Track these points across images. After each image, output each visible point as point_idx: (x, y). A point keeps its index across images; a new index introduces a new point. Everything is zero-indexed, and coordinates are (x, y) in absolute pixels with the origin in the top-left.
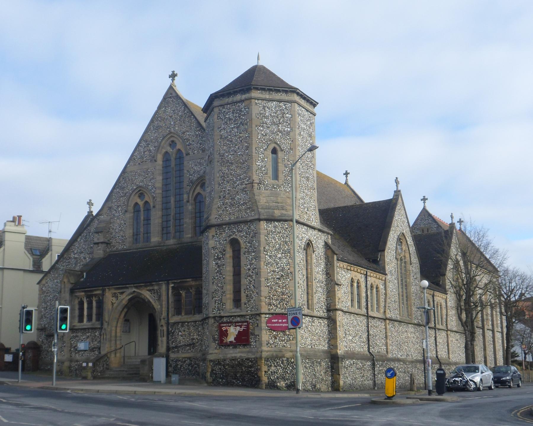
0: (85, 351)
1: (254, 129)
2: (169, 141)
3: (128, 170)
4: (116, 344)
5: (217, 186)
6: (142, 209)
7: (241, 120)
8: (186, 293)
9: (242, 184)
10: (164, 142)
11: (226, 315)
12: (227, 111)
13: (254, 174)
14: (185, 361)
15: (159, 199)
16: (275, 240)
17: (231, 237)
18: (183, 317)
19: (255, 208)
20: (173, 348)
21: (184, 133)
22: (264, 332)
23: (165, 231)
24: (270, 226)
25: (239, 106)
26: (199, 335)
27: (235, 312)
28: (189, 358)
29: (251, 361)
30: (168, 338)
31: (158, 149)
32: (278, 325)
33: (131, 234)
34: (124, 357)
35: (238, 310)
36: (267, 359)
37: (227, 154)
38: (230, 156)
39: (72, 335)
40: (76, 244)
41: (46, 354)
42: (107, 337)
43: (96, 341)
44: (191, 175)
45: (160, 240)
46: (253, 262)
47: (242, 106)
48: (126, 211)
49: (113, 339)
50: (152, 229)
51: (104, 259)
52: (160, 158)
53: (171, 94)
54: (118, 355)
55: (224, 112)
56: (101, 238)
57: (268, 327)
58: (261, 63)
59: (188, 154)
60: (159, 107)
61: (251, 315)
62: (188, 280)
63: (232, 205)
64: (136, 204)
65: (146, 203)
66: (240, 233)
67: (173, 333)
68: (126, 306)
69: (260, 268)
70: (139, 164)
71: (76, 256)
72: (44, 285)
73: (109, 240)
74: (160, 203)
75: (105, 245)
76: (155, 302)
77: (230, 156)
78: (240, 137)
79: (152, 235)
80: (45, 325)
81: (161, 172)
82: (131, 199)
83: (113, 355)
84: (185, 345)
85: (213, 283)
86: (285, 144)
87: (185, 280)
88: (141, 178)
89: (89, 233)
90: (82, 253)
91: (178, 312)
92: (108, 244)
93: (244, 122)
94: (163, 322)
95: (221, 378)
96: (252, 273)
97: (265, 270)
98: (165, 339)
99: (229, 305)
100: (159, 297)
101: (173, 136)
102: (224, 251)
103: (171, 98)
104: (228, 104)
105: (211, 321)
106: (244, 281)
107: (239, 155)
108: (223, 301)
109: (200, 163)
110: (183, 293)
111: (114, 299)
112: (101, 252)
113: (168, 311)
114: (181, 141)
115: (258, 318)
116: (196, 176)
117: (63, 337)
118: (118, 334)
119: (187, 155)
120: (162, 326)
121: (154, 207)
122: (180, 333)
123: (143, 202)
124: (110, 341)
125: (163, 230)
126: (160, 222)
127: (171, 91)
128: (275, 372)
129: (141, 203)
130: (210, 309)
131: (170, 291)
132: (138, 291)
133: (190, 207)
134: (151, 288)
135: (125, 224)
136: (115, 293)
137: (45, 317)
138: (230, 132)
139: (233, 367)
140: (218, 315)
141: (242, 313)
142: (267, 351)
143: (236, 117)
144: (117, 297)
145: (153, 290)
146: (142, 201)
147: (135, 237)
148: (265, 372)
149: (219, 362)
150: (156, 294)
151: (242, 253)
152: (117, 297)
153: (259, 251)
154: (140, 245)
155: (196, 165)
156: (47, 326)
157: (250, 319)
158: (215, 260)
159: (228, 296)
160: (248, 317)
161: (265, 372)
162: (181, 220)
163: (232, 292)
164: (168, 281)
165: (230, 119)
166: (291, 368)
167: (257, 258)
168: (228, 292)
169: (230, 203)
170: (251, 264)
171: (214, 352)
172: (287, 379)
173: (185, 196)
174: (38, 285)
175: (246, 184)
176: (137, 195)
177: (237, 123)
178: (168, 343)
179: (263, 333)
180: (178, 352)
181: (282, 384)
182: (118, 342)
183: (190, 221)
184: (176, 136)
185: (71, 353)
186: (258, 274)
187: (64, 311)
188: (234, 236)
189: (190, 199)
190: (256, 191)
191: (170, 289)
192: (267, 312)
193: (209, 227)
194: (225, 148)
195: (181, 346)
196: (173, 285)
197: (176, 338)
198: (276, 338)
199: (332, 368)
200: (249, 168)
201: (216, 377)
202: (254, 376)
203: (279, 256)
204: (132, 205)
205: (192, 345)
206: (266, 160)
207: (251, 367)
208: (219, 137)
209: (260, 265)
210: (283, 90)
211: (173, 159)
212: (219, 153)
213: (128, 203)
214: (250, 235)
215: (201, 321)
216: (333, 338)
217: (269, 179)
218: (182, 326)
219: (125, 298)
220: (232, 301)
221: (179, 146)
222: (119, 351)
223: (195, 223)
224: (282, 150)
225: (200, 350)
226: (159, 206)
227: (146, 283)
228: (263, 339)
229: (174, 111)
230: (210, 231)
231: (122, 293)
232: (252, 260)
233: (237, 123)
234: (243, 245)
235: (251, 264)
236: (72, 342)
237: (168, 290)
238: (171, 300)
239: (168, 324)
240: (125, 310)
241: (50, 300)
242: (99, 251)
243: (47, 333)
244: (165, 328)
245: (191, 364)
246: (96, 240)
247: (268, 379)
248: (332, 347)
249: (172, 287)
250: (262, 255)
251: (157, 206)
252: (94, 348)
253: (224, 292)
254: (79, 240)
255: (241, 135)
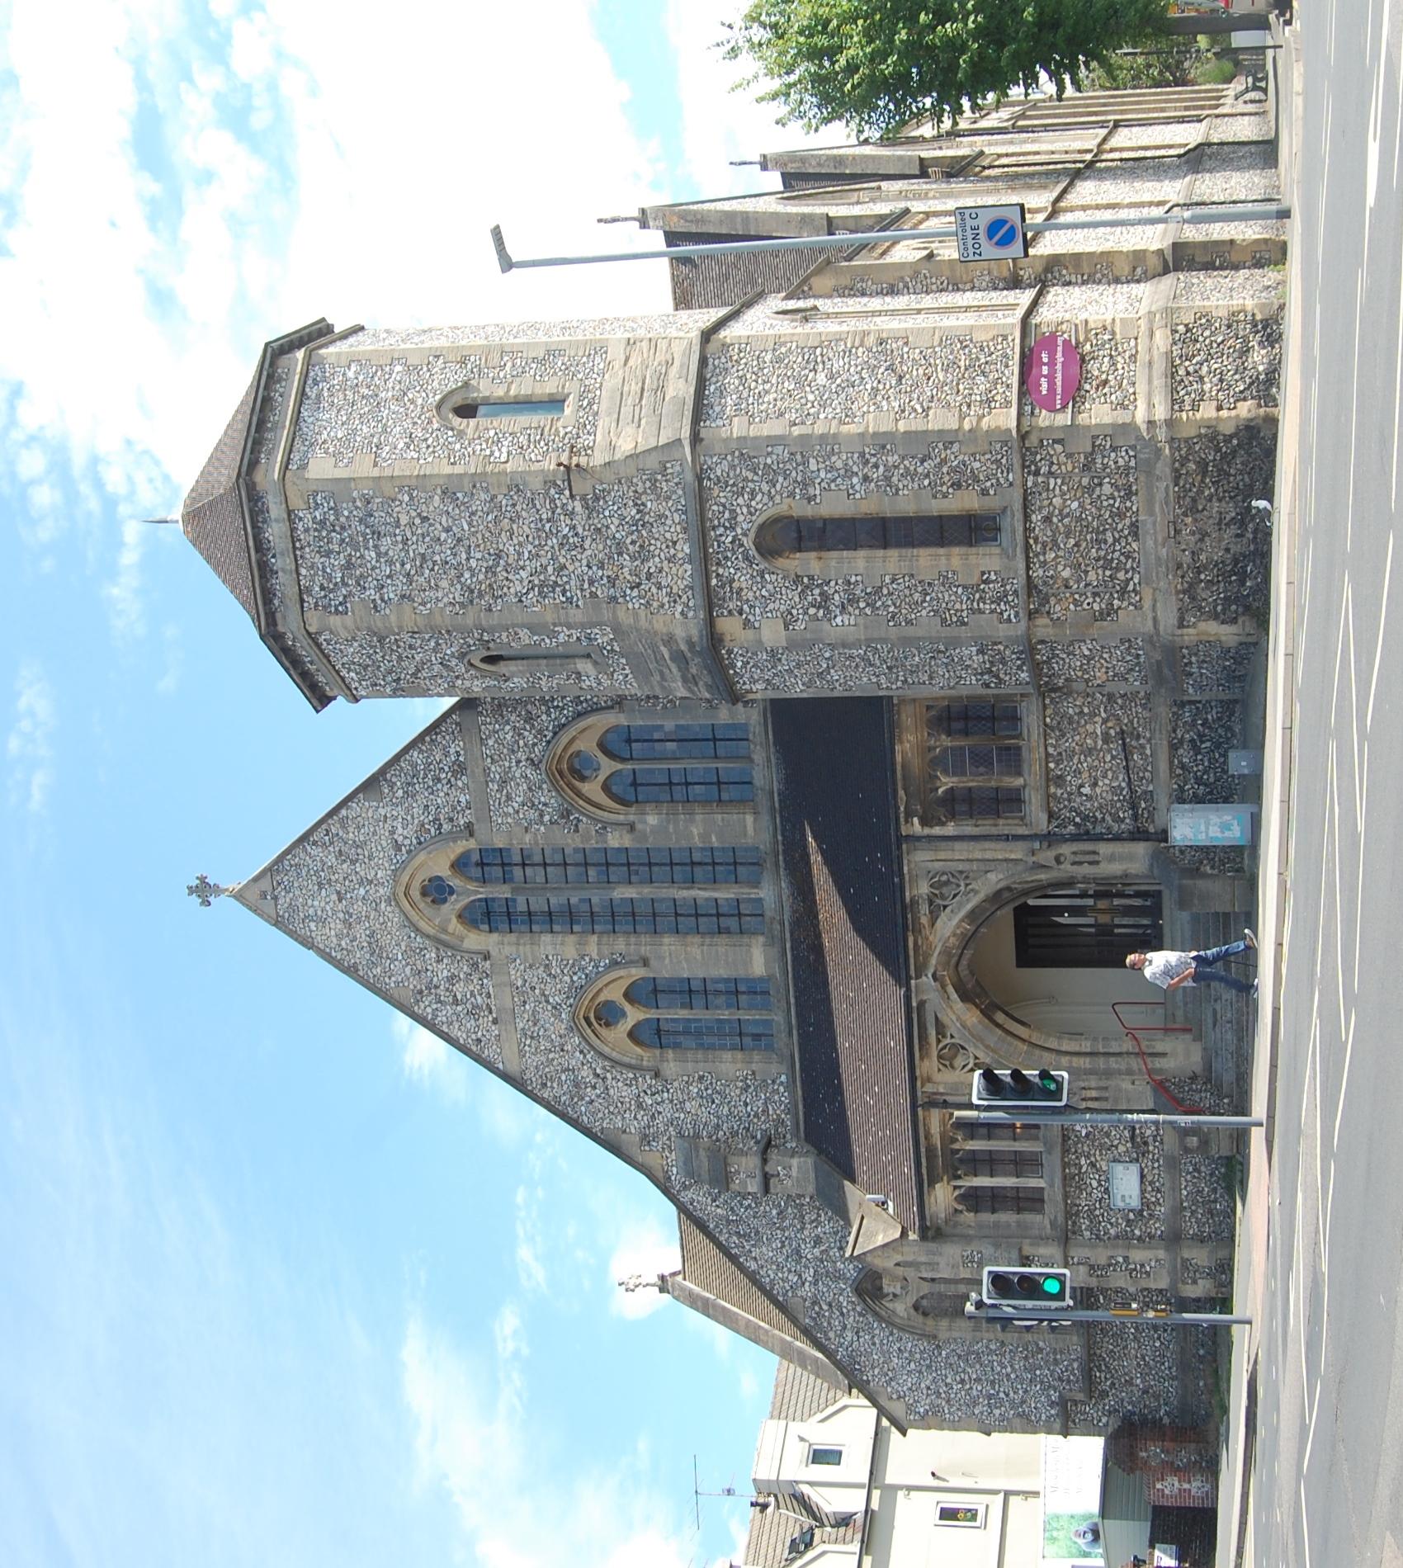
0: (1142, 1176)
1: (387, 473)
2: (422, 905)
3: (513, 1068)
4: (1120, 1054)
5: (572, 611)
6: (652, 1014)
7: (355, 523)
8: (946, 772)
9: (571, 514)
10: (422, 925)
11: (1022, 565)
12: (319, 579)
13: (535, 467)
14: (1183, 766)
15: (620, 944)
16: (767, 392)
17: (753, 552)
18: (1029, 782)
19: (652, 463)
20: (1135, 817)
21: (398, 847)
22: (1083, 419)
23: (724, 791)
24: (717, 409)
25: (307, 530)
26: (1093, 715)
27: (1014, 532)
28: (1173, 748)
29: (1184, 461)
30: (1099, 838)
31: (447, 945)
32: (1059, 375)
33: (739, 1055)
34: (1166, 1030)
35: (1005, 523)
36: (1175, 402)
37: (467, 575)
38: (473, 563)
39: (1087, 1234)
40: (769, 1274)
41: (1157, 1397)
42: (1093, 1084)
43: (1108, 1135)
44: (541, 816)
45: (761, 939)
46: (839, 464)
47: (306, 519)
48: (657, 1075)
49: (1101, 1063)
50: (723, 972)
51: (820, 1151)
52: (476, 940)
53: (264, 895)
54: (1160, 1047)
55: (322, 588)
56: (745, 1168)
57: (1064, 407)
58: (177, 513)
59: (470, 830)
60: (307, 943)
61: (1024, 467)
62: (899, 758)
63: (643, 554)
64: (632, 1035)
65: (626, 995)
66: (740, 518)
67: (1085, 818)
68: (987, 1013)
69: (862, 435)
70: (495, 1021)
71: (808, 1276)
72: (909, 1407)
73: (757, 1142)
74: (633, 939)
75: (773, 1155)
76: (976, 892)
77: (473, 563)
78: (411, 524)
79: (741, 973)
80: (1052, 1404)
81: (527, 937)
82: (614, 1054)
83: (1159, 1063)
84: (1127, 768)
85: (909, 622)
86: (446, 380)
87: (899, 768)
88: (546, 1016)
89: (729, 1222)
90: (798, 1252)
91: (1012, 801)
92: (767, 1146)
93: (359, 514)
94: (1047, 856)
95: (1242, 583)
96: (876, 466)
97: (874, 418)
98: (1104, 849)
99: (986, 559)
100: (958, 874)
101: (408, 887)
102: (798, 579)
103: (275, 898)
104: (298, 574)
105: (1043, 628)
106: (907, 502)
107: (470, 524)
108: (975, 580)
109: (504, 782)
110: (946, 783)
111: (959, 1061)
112: (795, 1162)
113: (1007, 838)
114: (422, 857)
115: (1033, 441)
116: (546, 796)
117: (1092, 1267)
118: (1086, 1046)
119: (471, 835)
120: (1058, 860)
121: (645, 963)
122: (1086, 790)
123: (627, 1007)
124: (1108, 1074)
125: (728, 932)
126: (697, 939)
127: (253, 895)
128: (1221, 381)
129: (634, 1015)
130: (1003, 631)
131: (937, 831)
132: (933, 961)
133: (652, 820)
134: (924, 908)
135: (701, 1078)
136: (940, 1057)
137: (1023, 1402)
138: (391, 563)
139: (1204, 535)
140: (1022, 593)
141: (1017, 505)
142: (1151, 406)
143: (343, 540)
144: (958, 1048)
145: (931, 903)
146: (624, 1014)
147: (747, 1040)
148: (1219, 408)
149: (1184, 592)
150: (945, 890)
151: (809, 511)
152: (958, 1048)
153: (803, 437)
154: (778, 1018)
155: (509, 798)
156: (1055, 1396)
157: (1037, 473)
158: (829, 617)
159: (956, 562)
160: (1030, 480)
161: (1219, 408)
162: (697, 857)
163: (941, 551)
164: (901, 839)
165: (349, 566)
166: (1207, 333)
167: (828, 443)
168: (943, 560)
169: (633, 558)
170: (849, 473)
171: (1150, 615)
172: (1246, 340)
173: (615, 840)
174: (910, 1432)
175: (572, 496)
176: (603, 1031)
177: (364, 535)
178: (1117, 838)
179: (1087, 422)
180: (1149, 796)
181: (1259, 358)
182: (1115, 1048)
183: (698, 818)
184: (405, 878)
185: (1151, 1237)
186: (883, 442)
187: (998, 1280)
188: (748, 542)
189: (622, 817)
190: (599, 458)
191: (927, 831)
192: (1014, 411)
193: (714, 639)
194: (444, 584)
195: (1129, 783)
196: (916, 820)
197: (1101, 807)
198: (1106, 382)
199: (1209, 266)
200: (516, 486)
201: (1236, 601)
202: (1234, 452)
203: (821, 378)
204: (638, 1050)
205: (1126, 740)
206: (492, 433)
207: (1203, 465)
208: (406, 604)
209: (850, 436)
210: (266, 388)
211: (483, 892)
212: (462, 605)
213: (630, 1067)
214: (746, 479)
215: (1045, 707)
216: (1110, 265)
217: (560, 424)
218: (1060, 780)
219: (960, 1016)
220: (974, 550)
221: (442, 869)
222: (1144, 1044)
223: (706, 802)
224: (466, 384)
225: (1144, 706)
226: (643, 945)
227: (905, 927)
228: (1107, 420)
229: (320, 884)
230: (728, 638)
231: (941, 1029)
232: (832, 468)
233: (364, 535)
234: (784, 506)
235: (849, 473)
236: (1112, 1232)
237: (930, 838)
238: (969, 829)
239: (1049, 839)
240: (1000, 1017)
241: (962, 1381)
242: (794, 1172)
243: (1080, 1396)
244: (1066, 849)
245: (1192, 741)
246: (753, 1187)
247: (1245, 399)
248: (1139, 271)
249: (924, 822)
250: (819, 429)
251: (644, 950)
252: (1133, 1137)
253: (946, 581)
254: (753, 1266)
255: (404, 520)
